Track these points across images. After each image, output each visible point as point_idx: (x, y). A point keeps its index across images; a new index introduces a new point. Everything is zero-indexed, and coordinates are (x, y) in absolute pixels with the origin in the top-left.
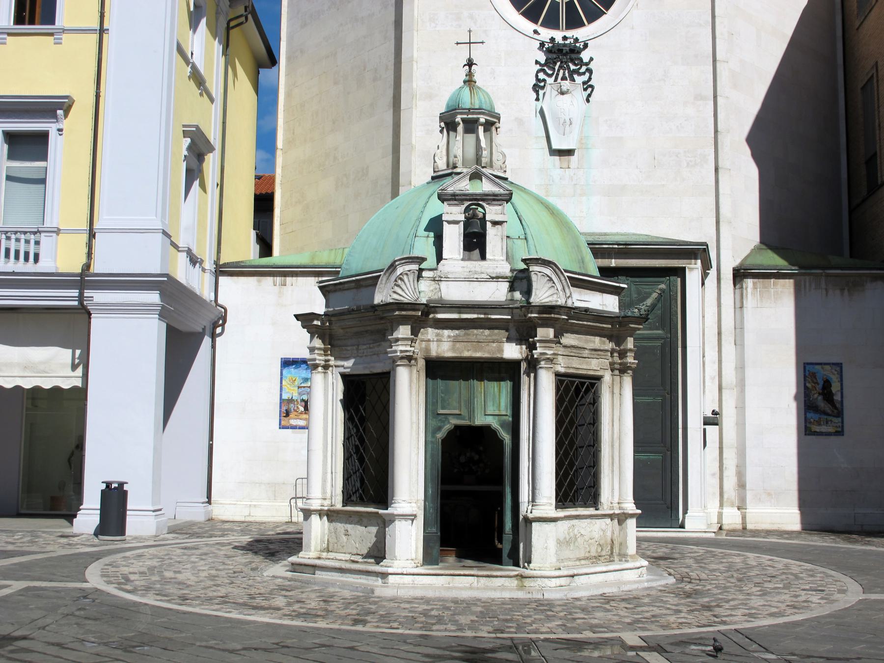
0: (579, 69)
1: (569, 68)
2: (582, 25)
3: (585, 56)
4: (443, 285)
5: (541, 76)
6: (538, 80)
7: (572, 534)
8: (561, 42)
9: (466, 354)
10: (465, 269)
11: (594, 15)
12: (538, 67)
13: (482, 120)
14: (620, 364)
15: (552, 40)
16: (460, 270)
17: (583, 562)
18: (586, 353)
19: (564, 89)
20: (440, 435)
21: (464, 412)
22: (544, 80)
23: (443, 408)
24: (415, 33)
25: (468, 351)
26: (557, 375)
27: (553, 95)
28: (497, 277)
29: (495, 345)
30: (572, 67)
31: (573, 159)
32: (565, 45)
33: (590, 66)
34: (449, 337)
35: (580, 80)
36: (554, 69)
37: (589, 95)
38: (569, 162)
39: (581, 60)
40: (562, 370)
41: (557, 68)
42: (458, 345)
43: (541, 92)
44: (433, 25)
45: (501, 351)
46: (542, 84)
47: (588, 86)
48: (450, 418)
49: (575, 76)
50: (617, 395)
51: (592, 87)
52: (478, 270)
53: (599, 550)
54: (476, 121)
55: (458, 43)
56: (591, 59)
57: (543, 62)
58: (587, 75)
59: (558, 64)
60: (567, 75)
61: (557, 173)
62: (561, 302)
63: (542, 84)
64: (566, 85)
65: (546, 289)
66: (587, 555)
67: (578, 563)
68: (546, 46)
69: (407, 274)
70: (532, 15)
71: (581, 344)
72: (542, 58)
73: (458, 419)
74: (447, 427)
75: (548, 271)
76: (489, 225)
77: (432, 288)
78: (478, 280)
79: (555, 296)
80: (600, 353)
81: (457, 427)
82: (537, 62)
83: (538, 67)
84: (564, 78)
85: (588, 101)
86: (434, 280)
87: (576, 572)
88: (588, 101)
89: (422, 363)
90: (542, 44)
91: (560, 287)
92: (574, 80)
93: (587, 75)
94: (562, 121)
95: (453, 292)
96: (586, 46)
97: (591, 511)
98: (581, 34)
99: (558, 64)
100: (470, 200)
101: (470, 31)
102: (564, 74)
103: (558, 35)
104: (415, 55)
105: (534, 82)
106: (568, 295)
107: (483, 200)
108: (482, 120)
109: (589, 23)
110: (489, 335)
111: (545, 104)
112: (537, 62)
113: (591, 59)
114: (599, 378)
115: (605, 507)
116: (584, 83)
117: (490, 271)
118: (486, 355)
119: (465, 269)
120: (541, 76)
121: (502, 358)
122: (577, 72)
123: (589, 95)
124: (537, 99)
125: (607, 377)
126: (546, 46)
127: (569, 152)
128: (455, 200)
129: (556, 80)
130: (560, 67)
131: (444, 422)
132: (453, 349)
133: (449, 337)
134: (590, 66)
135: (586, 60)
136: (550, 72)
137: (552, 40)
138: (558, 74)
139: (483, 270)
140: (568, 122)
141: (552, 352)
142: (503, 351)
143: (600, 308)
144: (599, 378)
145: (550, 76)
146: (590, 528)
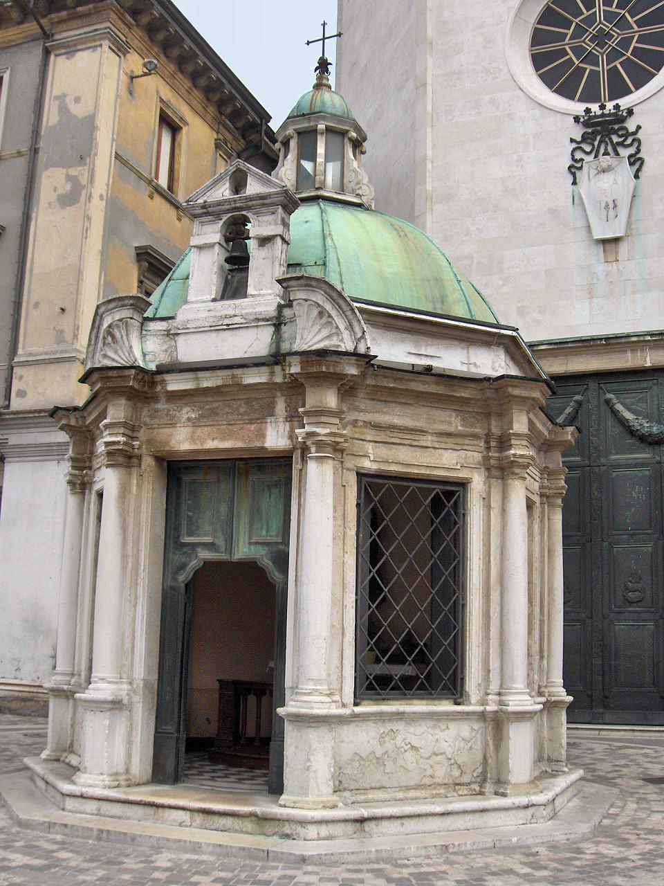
0: (624, 140)
1: (612, 142)
2: (629, 92)
3: (631, 125)
4: (181, 341)
5: (578, 155)
6: (573, 159)
7: (389, 746)
8: (599, 112)
9: (210, 445)
10: (212, 314)
11: (641, 79)
12: (574, 145)
13: (321, 127)
14: (498, 459)
15: (588, 111)
16: (206, 314)
17: (412, 794)
18: (428, 440)
19: (604, 165)
20: (182, 578)
21: (220, 541)
22: (582, 160)
23: (190, 534)
24: (429, 130)
25: (213, 439)
26: (360, 475)
27: (591, 176)
28: (258, 320)
29: (253, 427)
30: (615, 139)
31: (623, 247)
32: (603, 115)
33: (638, 136)
34: (189, 419)
35: (625, 153)
36: (593, 145)
37: (638, 170)
38: (617, 253)
39: (626, 129)
40: (369, 465)
41: (596, 143)
42: (199, 431)
43: (578, 174)
44: (449, 117)
45: (262, 435)
46: (579, 165)
47: (636, 161)
48: (199, 549)
49: (621, 150)
50: (495, 514)
51: (640, 159)
52: (231, 312)
53: (456, 773)
54: (314, 132)
55: (308, 43)
56: (639, 127)
57: (579, 139)
58: (636, 145)
59: (598, 138)
60: (610, 149)
61: (601, 268)
62: (348, 346)
63: (579, 165)
64: (605, 161)
65: (317, 327)
66: (427, 781)
67: (400, 795)
68: (582, 120)
69: (118, 326)
70: (566, 91)
71: (420, 424)
72: (577, 132)
73: (211, 550)
74: (194, 564)
75: (319, 297)
76: (252, 245)
77: (165, 347)
78: (229, 328)
79: (335, 338)
80: (459, 440)
81: (208, 564)
82: (572, 140)
83: (574, 145)
84: (606, 153)
85: (636, 177)
86: (168, 335)
87: (365, 813)
88: (636, 177)
89: (148, 462)
90: (577, 119)
91: (342, 325)
92: (617, 154)
93: (636, 145)
94: (603, 206)
95: (192, 350)
96: (630, 112)
97: (446, 706)
98: (624, 102)
99: (598, 138)
100: (228, 211)
101: (324, 25)
102: (606, 149)
103: (595, 108)
104: (429, 153)
105: (569, 162)
106: (359, 335)
107: (248, 208)
108: (321, 127)
109: (637, 89)
110: (245, 413)
111: (583, 188)
112: (572, 140)
113: (639, 127)
114: (463, 484)
115: (474, 699)
116: (630, 157)
117: (244, 312)
118: (239, 445)
119: (212, 314)
120: (578, 155)
121: (263, 448)
122: (621, 144)
123: (638, 170)
124: (574, 183)
125: (478, 483)
126: (582, 120)
127: (616, 240)
128: (208, 214)
129: (596, 157)
130: (600, 142)
131: (189, 556)
132: (192, 439)
133: (189, 419)
134: (638, 136)
135: (632, 128)
136: (588, 149)
137: (588, 111)
138: (598, 151)
139: (237, 312)
140: (611, 205)
141: (327, 431)
142: (264, 436)
143: (464, 368)
144: (463, 484)
145: (588, 153)
146: (428, 735)
